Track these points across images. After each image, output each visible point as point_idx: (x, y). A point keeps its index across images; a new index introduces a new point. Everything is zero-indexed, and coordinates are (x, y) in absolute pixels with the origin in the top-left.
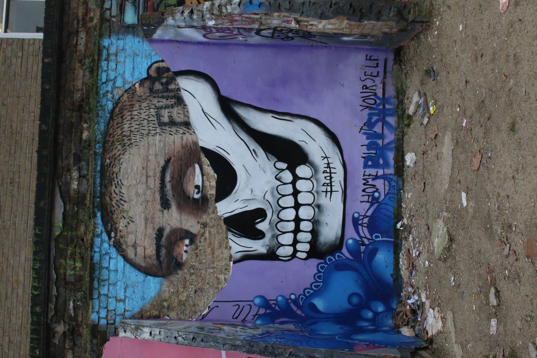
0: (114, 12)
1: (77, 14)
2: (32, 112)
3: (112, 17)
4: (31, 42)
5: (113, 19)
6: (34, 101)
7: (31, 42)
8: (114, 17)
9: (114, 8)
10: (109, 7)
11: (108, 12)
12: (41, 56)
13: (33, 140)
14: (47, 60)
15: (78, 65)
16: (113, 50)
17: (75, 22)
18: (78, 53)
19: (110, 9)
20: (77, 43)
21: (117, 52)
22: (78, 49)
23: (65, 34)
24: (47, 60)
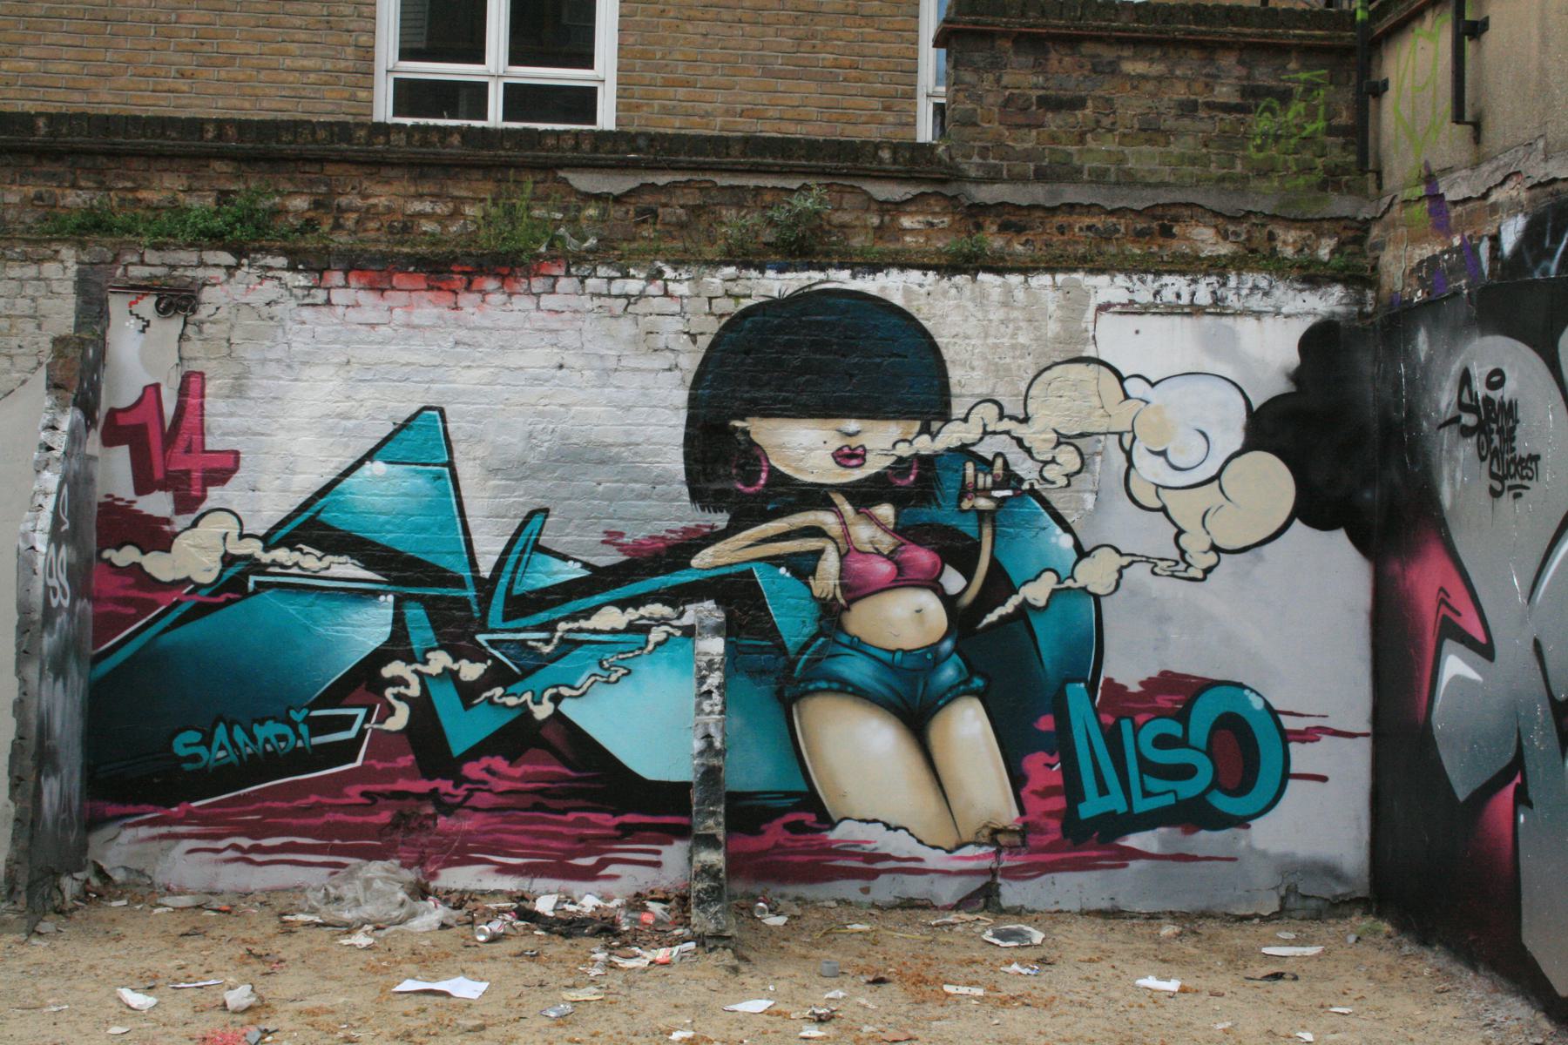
0: (137, 272)
1: (146, 188)
2: (179, 16)
3: (126, 266)
4: (365, 10)
5: (119, 272)
6: (207, 19)
7: (365, 10)
8: (126, 270)
9: (145, 271)
10: (147, 260)
11: (135, 259)
12: (51, 108)
13: (105, 19)
14: (41, 123)
15: (31, 191)
16: (50, 269)
17: (129, 184)
18: (58, 191)
19: (142, 263)
20: (81, 188)
21: (45, 279)
22: (68, 191)
23: (101, 160)
24: (41, 123)
